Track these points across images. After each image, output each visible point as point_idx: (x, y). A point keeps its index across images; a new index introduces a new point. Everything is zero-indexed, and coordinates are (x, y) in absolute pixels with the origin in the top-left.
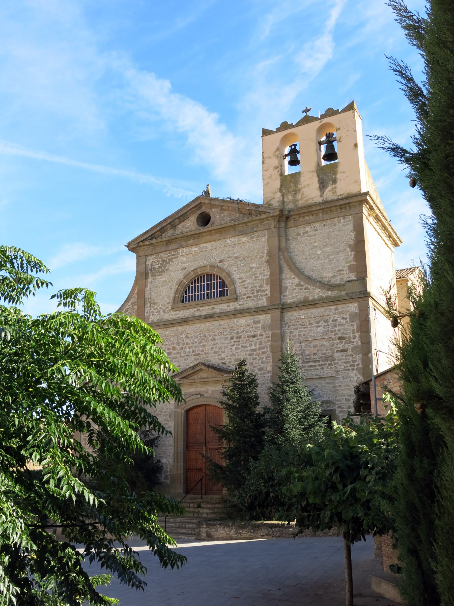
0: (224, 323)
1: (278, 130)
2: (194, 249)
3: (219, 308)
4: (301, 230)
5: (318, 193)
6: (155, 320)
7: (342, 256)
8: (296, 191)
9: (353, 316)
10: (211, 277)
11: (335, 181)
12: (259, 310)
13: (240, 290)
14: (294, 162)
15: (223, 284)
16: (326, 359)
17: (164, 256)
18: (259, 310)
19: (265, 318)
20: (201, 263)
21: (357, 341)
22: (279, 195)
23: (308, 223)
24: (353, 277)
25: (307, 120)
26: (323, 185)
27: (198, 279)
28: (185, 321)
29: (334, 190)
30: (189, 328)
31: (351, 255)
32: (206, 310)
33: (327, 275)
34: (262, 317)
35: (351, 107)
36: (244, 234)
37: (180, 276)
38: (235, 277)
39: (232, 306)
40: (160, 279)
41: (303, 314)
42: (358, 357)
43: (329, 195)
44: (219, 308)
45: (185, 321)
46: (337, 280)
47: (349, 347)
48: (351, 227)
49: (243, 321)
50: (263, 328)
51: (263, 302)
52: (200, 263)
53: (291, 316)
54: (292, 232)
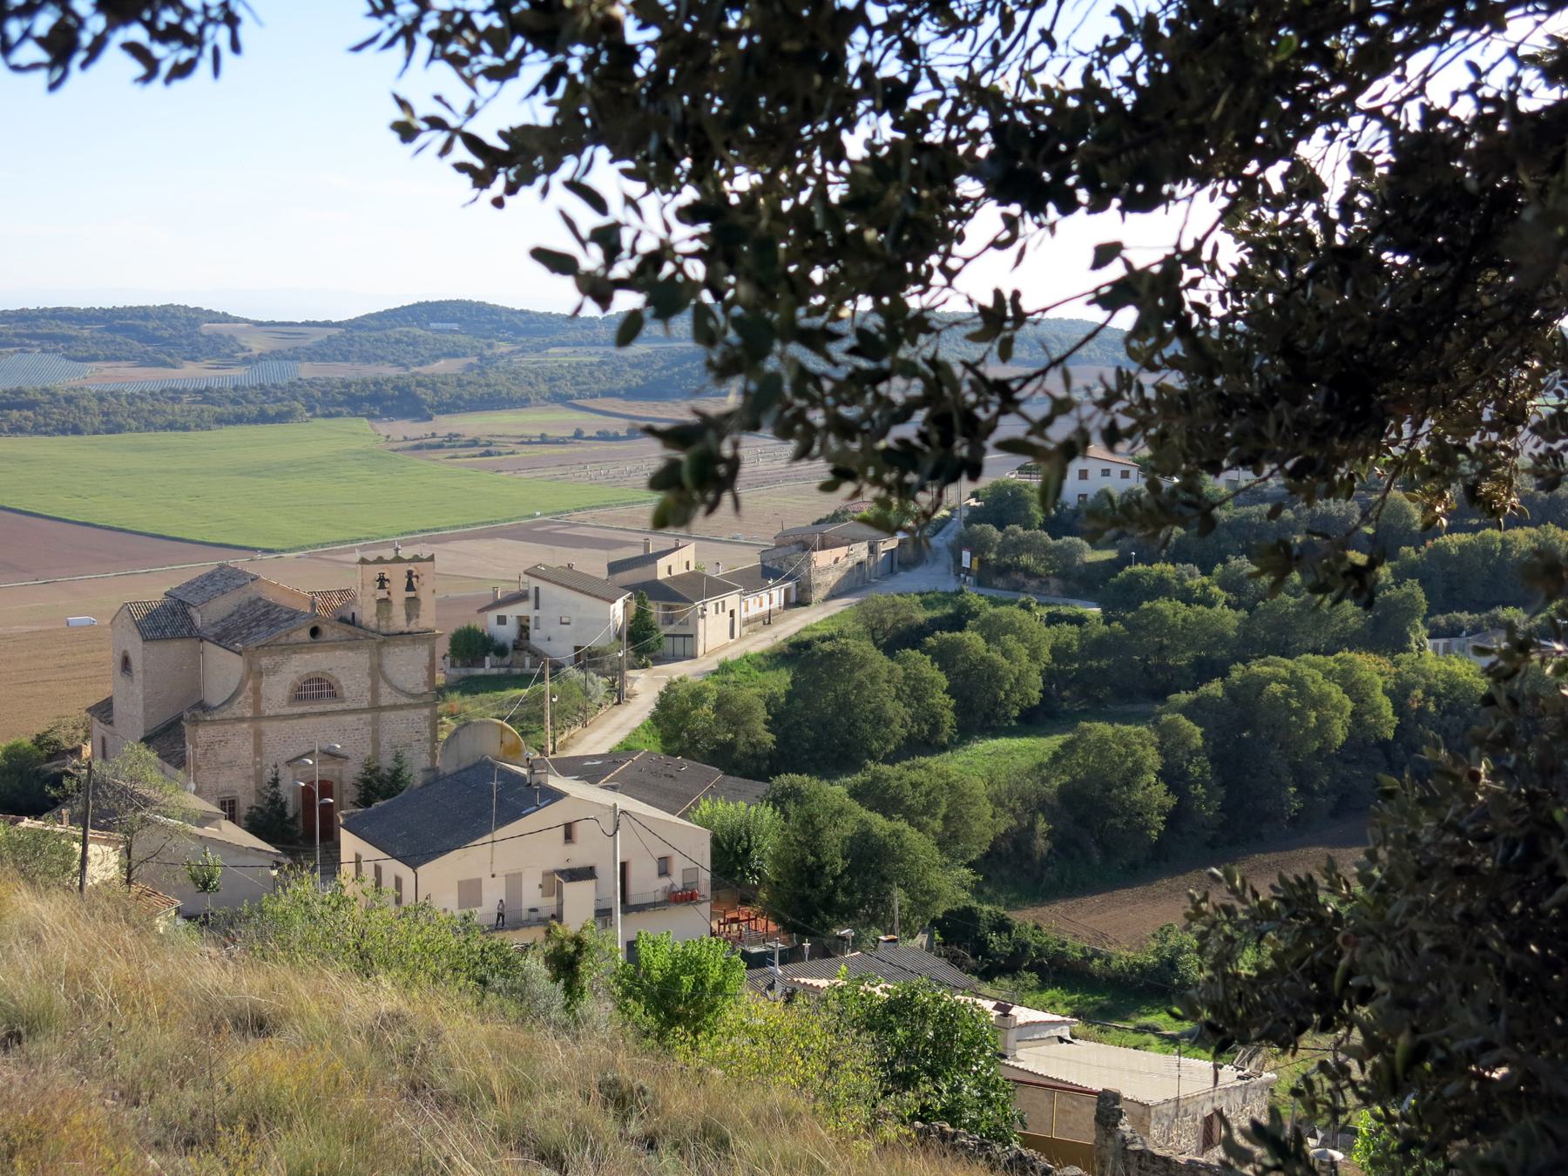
0: (334, 718)
1: (375, 562)
2: (307, 657)
3: (330, 707)
4: (391, 650)
5: (405, 623)
6: (272, 713)
7: (419, 674)
8: (389, 619)
9: (426, 718)
10: (319, 680)
11: (418, 617)
12: (363, 711)
13: (346, 694)
14: (382, 587)
15: (330, 686)
16: (406, 745)
17: (277, 659)
18: (363, 711)
19: (367, 717)
20: (314, 669)
21: (428, 735)
22: (375, 619)
23: (397, 645)
24: (426, 690)
25: (398, 560)
26: (409, 618)
27: (310, 681)
28: (302, 716)
29: (417, 623)
30: (302, 721)
31: (426, 673)
32: (318, 708)
33: (409, 686)
34: (364, 716)
35: (431, 558)
36: (350, 649)
37: (294, 677)
38: (343, 683)
39: (340, 707)
40: (273, 679)
41: (391, 715)
42: (428, 745)
43: (413, 627)
44: (330, 707)
45: (302, 716)
46: (415, 691)
47: (422, 738)
48: (426, 653)
49: (349, 718)
50: (365, 723)
51: (365, 705)
52: (311, 669)
53: (385, 715)
54: (385, 650)
